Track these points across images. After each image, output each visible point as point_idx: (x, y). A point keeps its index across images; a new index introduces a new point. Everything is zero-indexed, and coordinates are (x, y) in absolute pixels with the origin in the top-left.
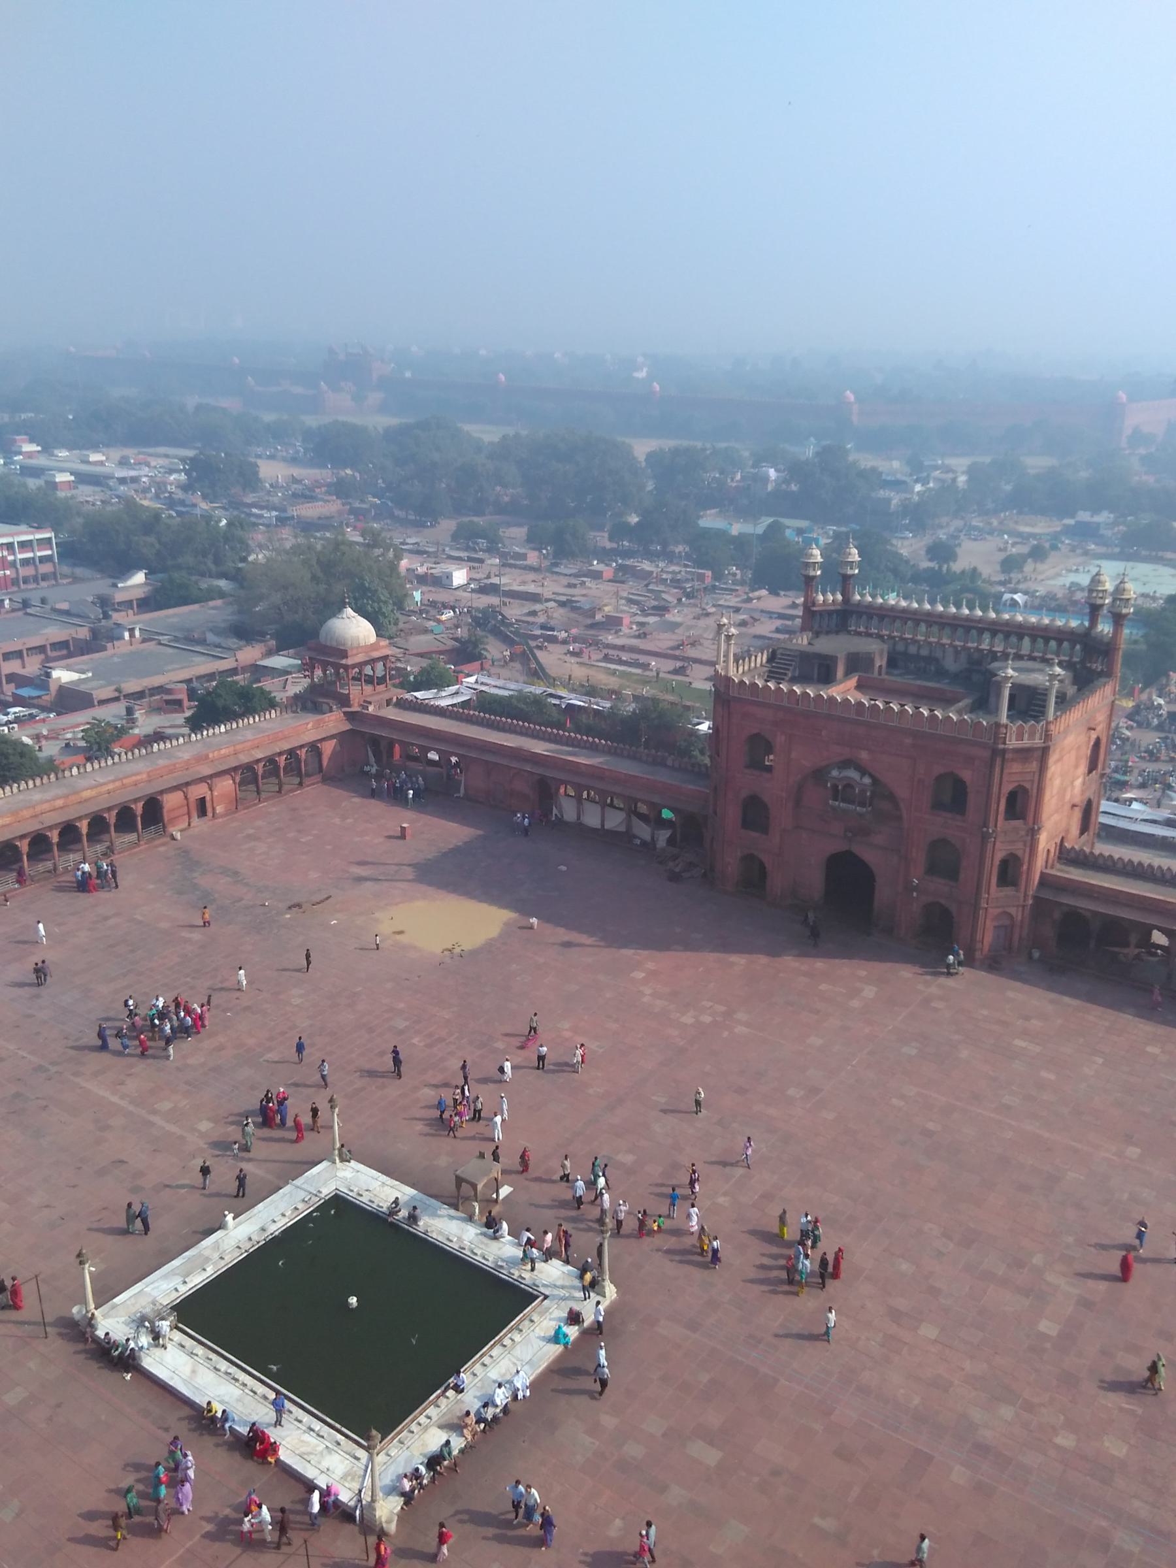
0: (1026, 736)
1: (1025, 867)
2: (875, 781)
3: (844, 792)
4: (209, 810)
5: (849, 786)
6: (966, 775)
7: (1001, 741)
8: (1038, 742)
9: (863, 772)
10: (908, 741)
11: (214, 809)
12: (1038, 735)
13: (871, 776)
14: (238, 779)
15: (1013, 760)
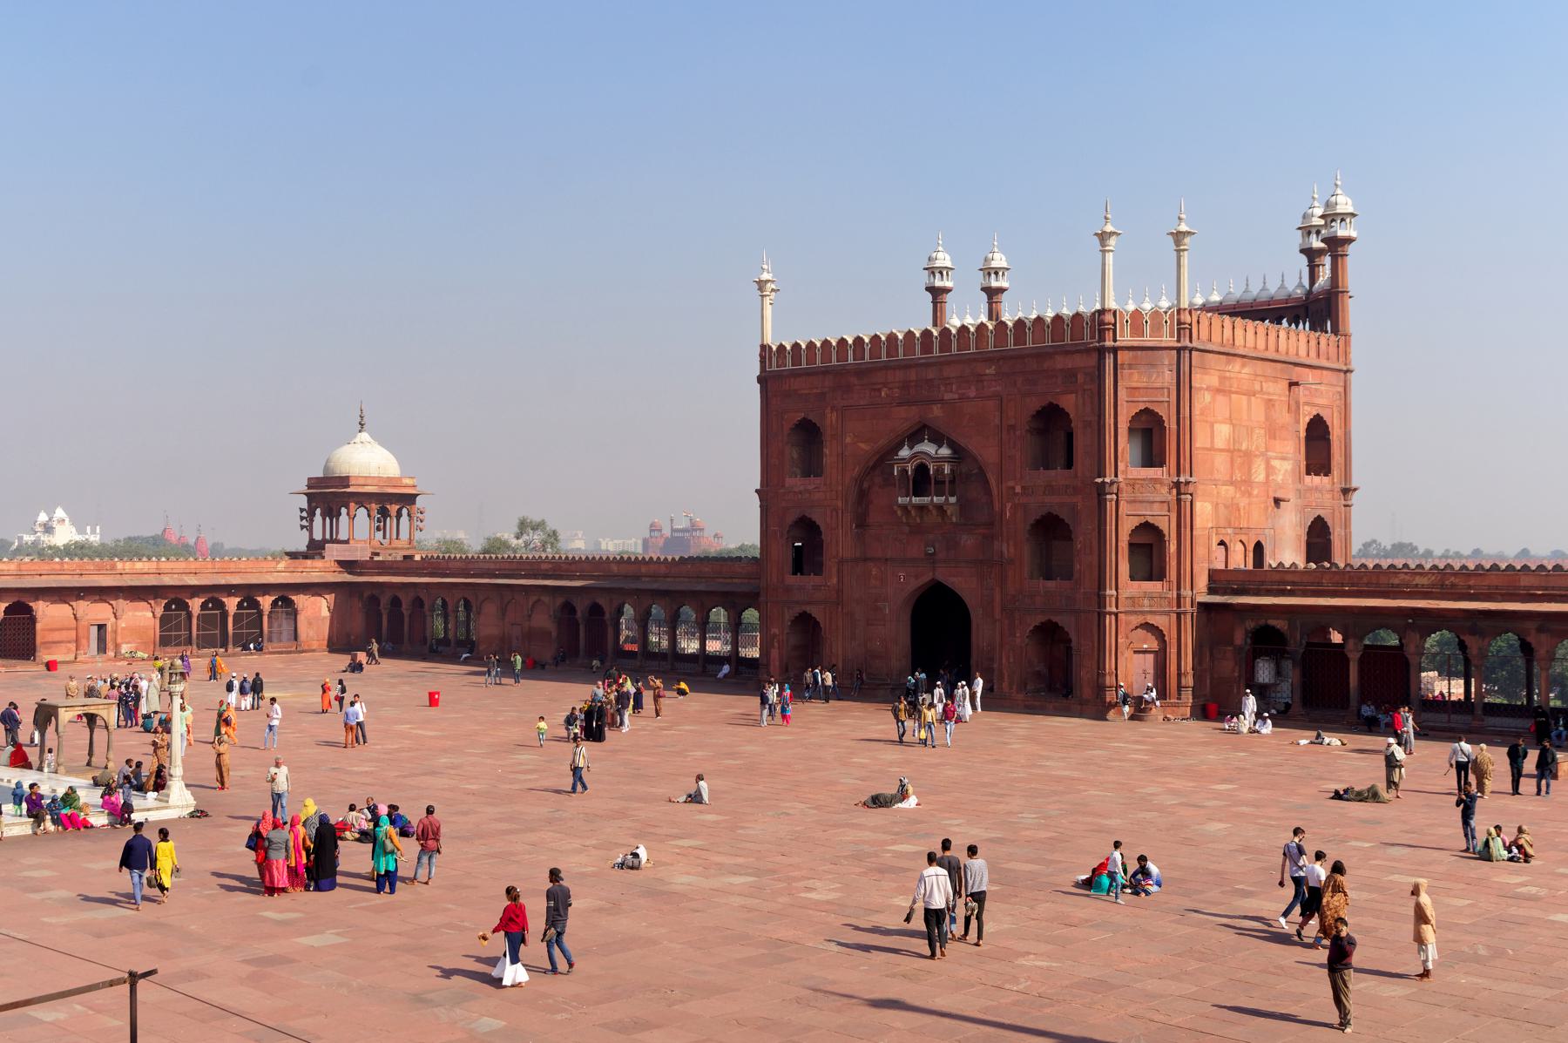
0: (1147, 329)
1: (1173, 548)
2: (959, 453)
3: (921, 480)
4: (110, 645)
5: (922, 470)
6: (1068, 403)
7: (1109, 335)
8: (1168, 340)
9: (938, 440)
10: (991, 371)
11: (117, 646)
12: (1166, 329)
13: (952, 445)
14: (159, 611)
15: (1130, 366)
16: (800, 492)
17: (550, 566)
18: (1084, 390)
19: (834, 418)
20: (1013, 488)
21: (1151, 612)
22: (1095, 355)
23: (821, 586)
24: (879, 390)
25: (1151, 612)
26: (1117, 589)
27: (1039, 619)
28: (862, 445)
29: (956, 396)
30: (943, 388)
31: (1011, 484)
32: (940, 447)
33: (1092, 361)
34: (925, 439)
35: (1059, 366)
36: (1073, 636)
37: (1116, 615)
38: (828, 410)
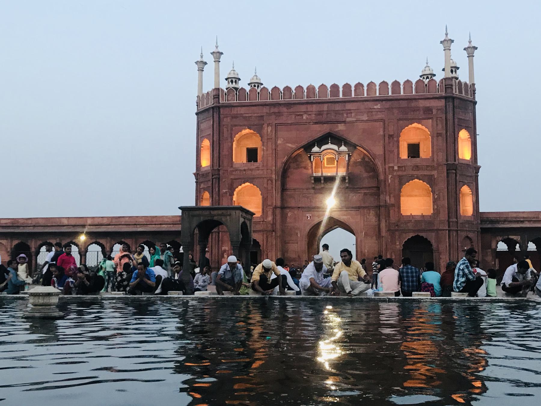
16: (245, 170)
17: (9, 221)
18: (437, 117)
19: (269, 131)
20: (393, 167)
21: (469, 231)
22: (443, 101)
23: (260, 222)
24: (302, 115)
25: (469, 231)
26: (457, 218)
27: (411, 235)
28: (290, 145)
29: (355, 119)
30: (345, 115)
31: (391, 165)
32: (339, 146)
33: (442, 103)
34: (329, 142)
35: (421, 105)
36: (433, 242)
37: (457, 231)
38: (265, 126)
